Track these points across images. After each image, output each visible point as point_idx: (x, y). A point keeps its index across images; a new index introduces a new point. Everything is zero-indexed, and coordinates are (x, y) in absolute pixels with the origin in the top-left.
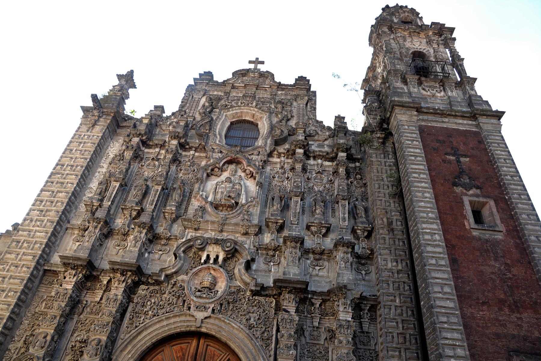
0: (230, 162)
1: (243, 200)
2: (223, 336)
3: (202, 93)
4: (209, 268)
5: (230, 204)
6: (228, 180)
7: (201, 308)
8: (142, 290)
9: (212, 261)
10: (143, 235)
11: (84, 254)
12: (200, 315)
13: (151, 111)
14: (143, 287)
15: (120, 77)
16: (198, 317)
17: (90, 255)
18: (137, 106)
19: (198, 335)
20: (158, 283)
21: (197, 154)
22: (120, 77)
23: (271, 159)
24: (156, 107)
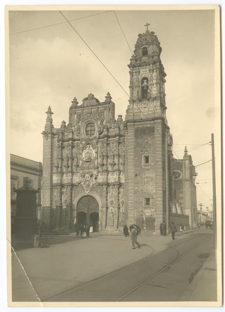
0: (87, 145)
1: (92, 158)
2: (93, 196)
3: (74, 113)
4: (87, 180)
5: (89, 161)
6: (88, 153)
7: (87, 190)
8: (74, 188)
9: (87, 178)
10: (70, 174)
11: (59, 182)
12: (87, 192)
13: (61, 125)
14: (74, 187)
15: (47, 113)
16: (87, 193)
17: (61, 181)
18: (57, 125)
19: (87, 196)
20: (78, 186)
21: (78, 142)
22: (47, 113)
23: (99, 140)
24: (62, 122)
